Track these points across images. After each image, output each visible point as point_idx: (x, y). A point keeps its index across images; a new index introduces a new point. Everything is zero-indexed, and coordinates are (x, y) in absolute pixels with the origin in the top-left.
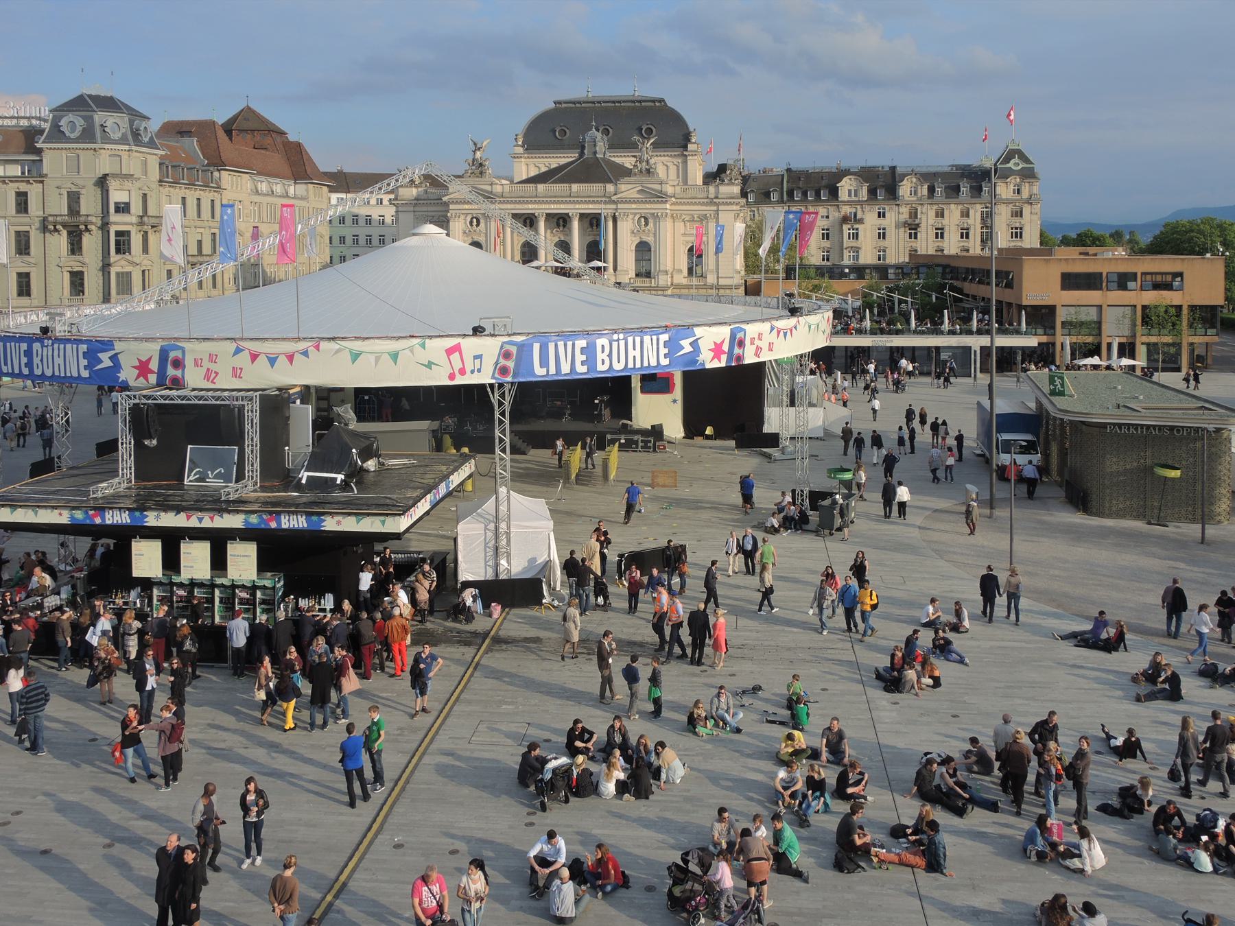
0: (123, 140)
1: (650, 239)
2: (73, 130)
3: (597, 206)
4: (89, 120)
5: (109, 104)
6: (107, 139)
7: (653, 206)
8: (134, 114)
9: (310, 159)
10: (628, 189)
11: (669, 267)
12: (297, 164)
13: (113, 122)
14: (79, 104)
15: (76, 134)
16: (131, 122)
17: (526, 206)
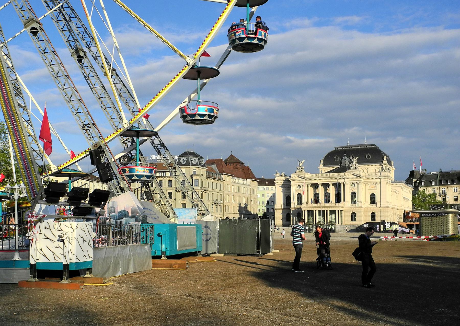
0: (197, 165)
1: (356, 191)
2: (184, 162)
3: (336, 180)
4: (188, 159)
5: (193, 154)
6: (192, 164)
7: (356, 179)
8: (200, 157)
9: (251, 172)
10: (348, 174)
11: (363, 201)
12: (247, 174)
13: (195, 160)
14: (185, 154)
15: (185, 163)
16: (199, 159)
17: (315, 181)
